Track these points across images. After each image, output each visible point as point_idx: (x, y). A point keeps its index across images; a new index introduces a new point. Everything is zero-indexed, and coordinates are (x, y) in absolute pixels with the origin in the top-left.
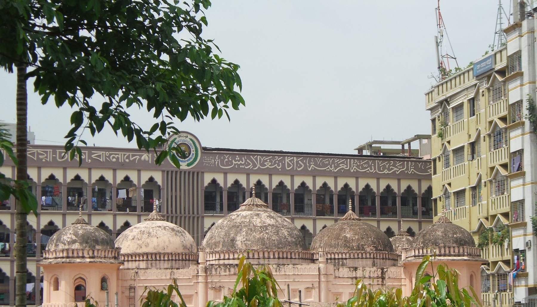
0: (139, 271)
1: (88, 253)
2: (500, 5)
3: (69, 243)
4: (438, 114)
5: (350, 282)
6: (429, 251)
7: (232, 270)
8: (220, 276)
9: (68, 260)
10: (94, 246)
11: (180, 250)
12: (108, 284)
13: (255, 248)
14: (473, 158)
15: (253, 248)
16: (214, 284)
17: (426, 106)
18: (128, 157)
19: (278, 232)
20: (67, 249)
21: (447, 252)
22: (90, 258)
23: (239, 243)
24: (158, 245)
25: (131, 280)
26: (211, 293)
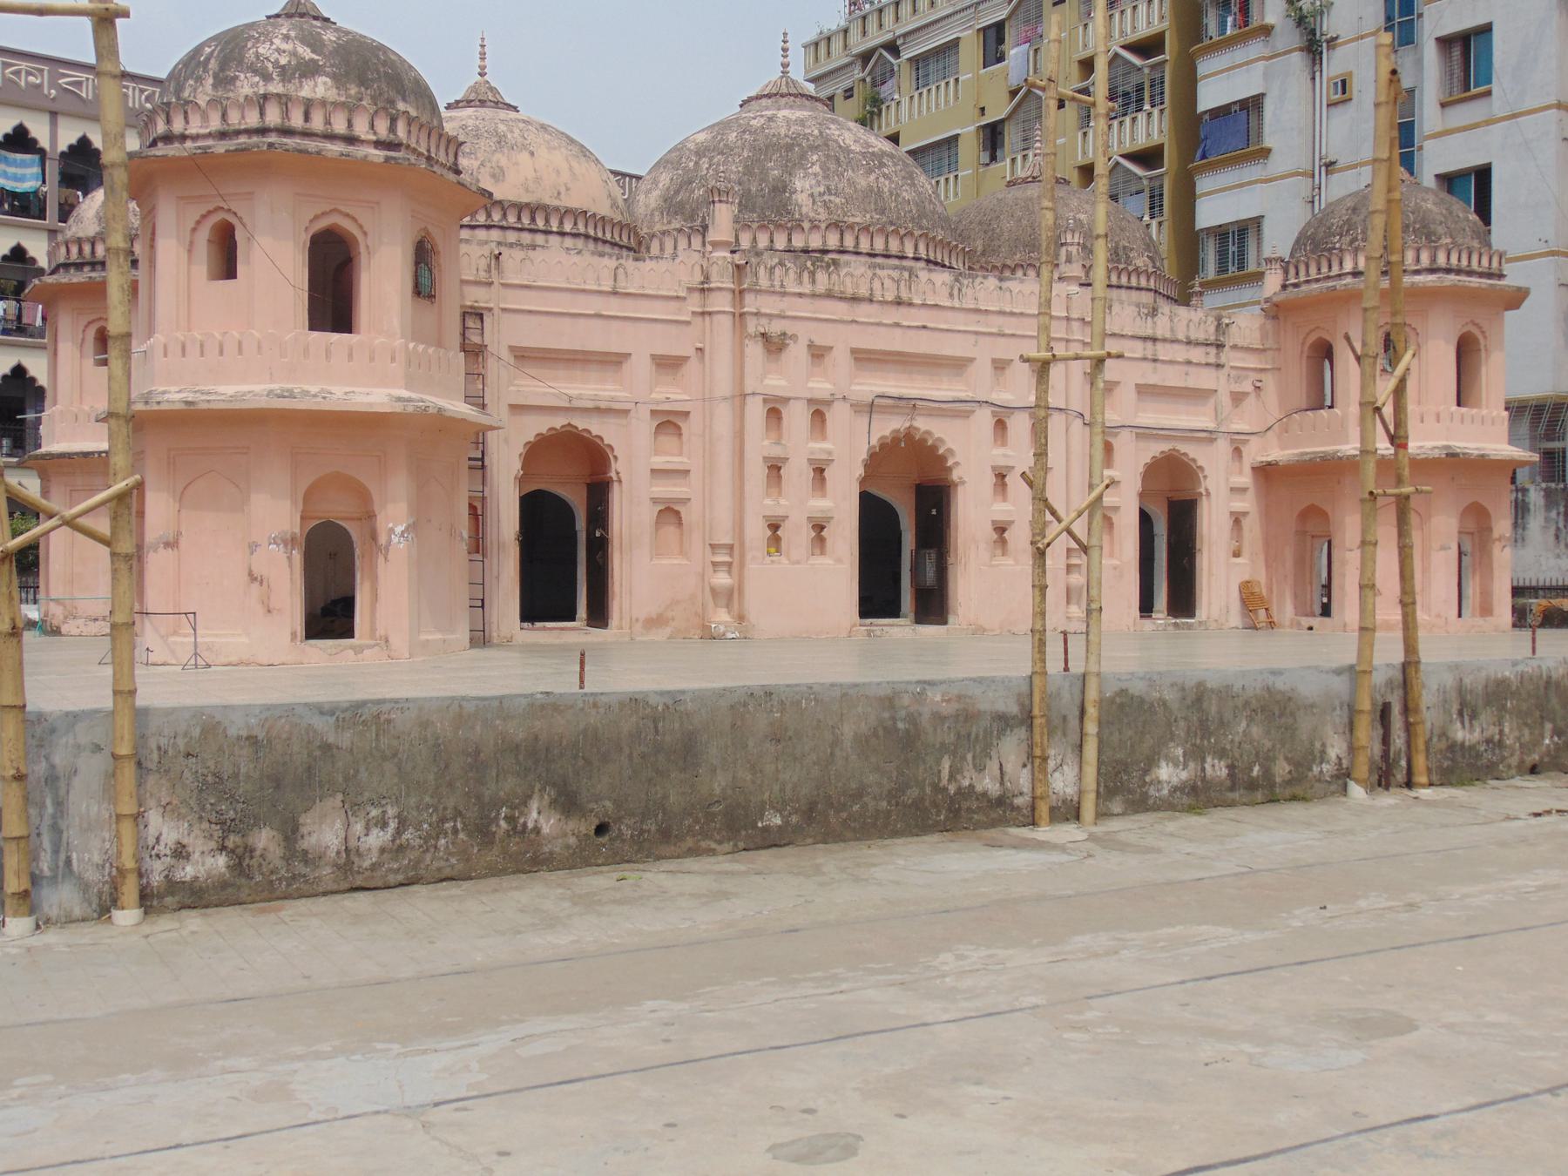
0: (505, 251)
1: (372, 126)
3: (285, 73)
4: (847, 84)
5: (1137, 349)
6: (1410, 256)
7: (821, 276)
8: (784, 294)
9: (290, 142)
10: (392, 102)
11: (604, 209)
12: (435, 271)
13: (858, 220)
14: (993, 158)
15: (851, 220)
16: (764, 321)
17: (806, 72)
18: (148, 99)
19: (912, 179)
20: (278, 95)
21: (1464, 262)
22: (378, 144)
23: (802, 198)
24: (538, 180)
25: (477, 283)
26: (755, 350)
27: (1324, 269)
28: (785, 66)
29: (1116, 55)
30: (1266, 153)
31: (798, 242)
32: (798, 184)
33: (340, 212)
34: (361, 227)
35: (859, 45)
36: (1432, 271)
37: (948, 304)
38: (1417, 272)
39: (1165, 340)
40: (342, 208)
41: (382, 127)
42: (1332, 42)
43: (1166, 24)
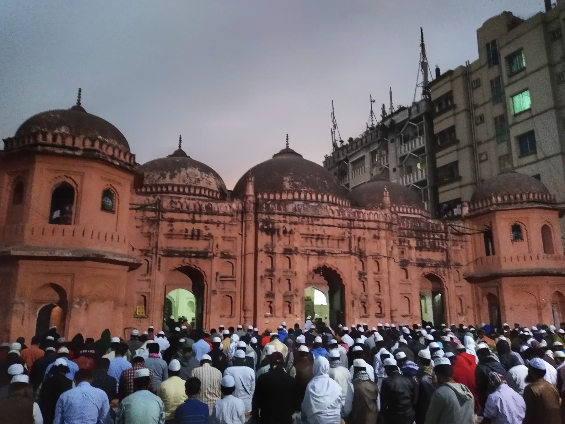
2: (372, 111)
8: (274, 214)
27: (485, 204)
28: (287, 144)
29: (410, 154)
30: (459, 178)
31: (284, 196)
32: (285, 178)
33: (67, 177)
34: (75, 182)
35: (337, 160)
36: (529, 202)
37: (338, 217)
38: (522, 203)
39: (423, 231)
40: (69, 176)
41: (88, 143)
42: (479, 143)
43: (425, 145)
